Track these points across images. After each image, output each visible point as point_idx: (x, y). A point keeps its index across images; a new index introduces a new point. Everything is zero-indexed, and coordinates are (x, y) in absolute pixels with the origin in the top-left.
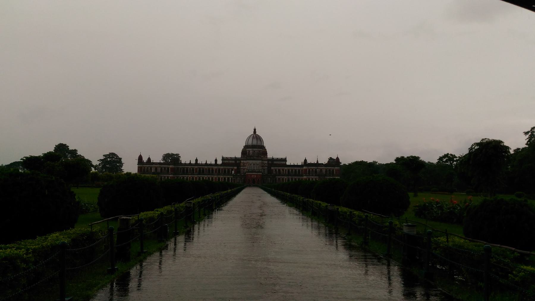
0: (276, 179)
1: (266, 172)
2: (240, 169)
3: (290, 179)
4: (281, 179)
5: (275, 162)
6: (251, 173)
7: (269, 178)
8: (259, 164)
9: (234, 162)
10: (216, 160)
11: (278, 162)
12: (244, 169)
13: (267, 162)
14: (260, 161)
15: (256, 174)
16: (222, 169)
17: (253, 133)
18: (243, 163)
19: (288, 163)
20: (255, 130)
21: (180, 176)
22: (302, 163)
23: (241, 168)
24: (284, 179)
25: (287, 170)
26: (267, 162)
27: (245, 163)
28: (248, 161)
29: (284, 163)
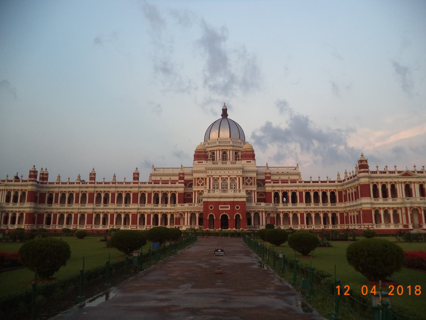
0: (278, 215)
1: (254, 196)
2: (192, 193)
3: (313, 215)
4: (291, 216)
7: (264, 214)
8: (236, 178)
9: (177, 178)
12: (200, 193)
16: (150, 194)
17: (221, 117)
18: (198, 178)
19: (304, 178)
22: (338, 175)
23: (194, 189)
24: (299, 215)
27: (202, 178)
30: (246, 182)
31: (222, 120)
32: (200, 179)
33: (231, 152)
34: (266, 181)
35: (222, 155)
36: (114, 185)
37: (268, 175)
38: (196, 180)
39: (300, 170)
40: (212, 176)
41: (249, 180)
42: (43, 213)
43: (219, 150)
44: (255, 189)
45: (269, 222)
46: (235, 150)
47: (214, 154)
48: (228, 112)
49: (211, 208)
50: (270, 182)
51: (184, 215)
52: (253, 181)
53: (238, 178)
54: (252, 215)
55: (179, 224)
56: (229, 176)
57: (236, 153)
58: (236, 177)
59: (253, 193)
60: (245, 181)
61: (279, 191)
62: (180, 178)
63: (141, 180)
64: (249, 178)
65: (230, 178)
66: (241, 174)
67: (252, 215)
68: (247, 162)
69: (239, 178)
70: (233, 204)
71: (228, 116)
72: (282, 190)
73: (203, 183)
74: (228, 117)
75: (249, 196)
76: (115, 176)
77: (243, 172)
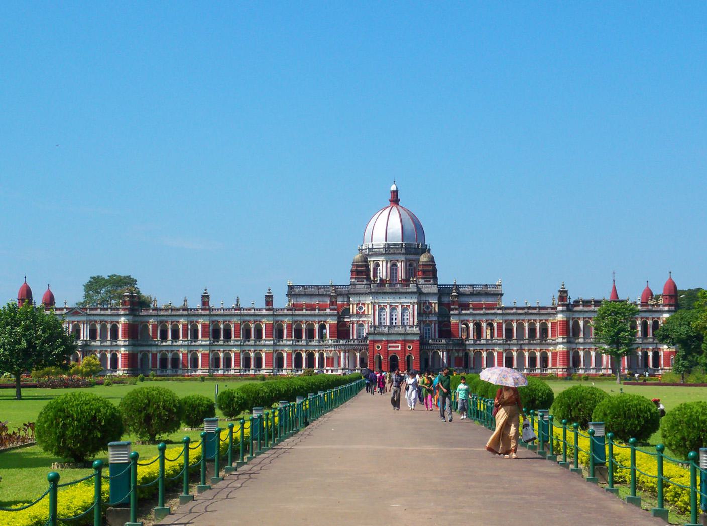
1: (434, 327)
10: (269, 299)
21: (154, 350)
22: (554, 299)
30: (424, 309)
31: (392, 208)
32: (360, 305)
34: (452, 307)
35: (390, 268)
36: (238, 312)
38: (355, 306)
41: (427, 306)
42: (136, 352)
44: (435, 318)
46: (410, 261)
47: (378, 265)
51: (340, 355)
53: (411, 306)
55: (333, 366)
57: (411, 265)
58: (409, 304)
59: (433, 324)
60: (422, 308)
62: (332, 303)
63: (276, 305)
64: (427, 303)
68: (425, 281)
71: (399, 200)
73: (364, 310)
76: (237, 300)
77: (419, 294)
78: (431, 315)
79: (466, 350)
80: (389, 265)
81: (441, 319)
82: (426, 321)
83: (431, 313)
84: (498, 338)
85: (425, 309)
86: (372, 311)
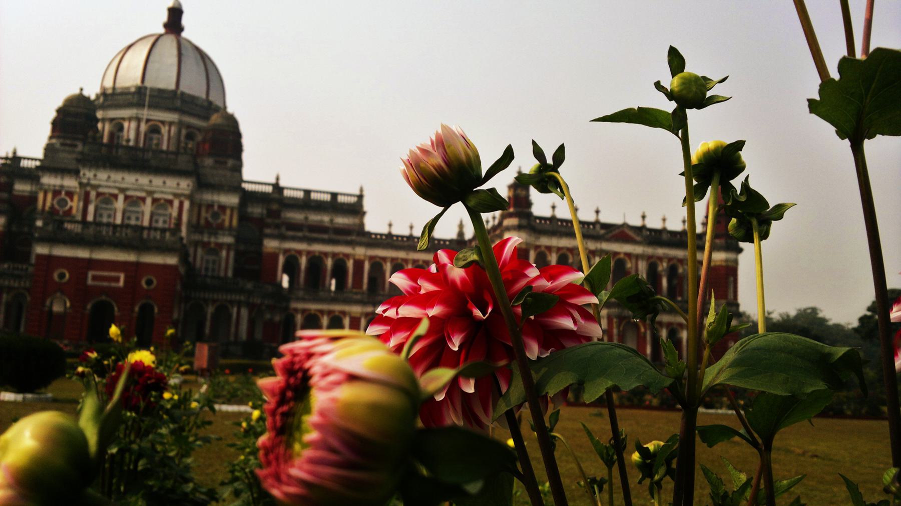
1: (226, 262)
5: (297, 216)
6: (83, 253)
8: (170, 202)
11: (315, 217)
13: (232, 200)
14: (185, 185)
15: (130, 257)
17: (162, 30)
18: (56, 193)
19: (374, 224)
20: (175, 15)
22: (461, 226)
25: (367, 266)
26: (232, 200)
27: (70, 194)
28: (88, 174)
29: (342, 220)
33: (174, 129)
37: (275, 207)
38: (50, 196)
39: (367, 205)
40: (95, 187)
43: (139, 120)
45: (259, 335)
47: (121, 128)
48: (185, 21)
49: (62, 276)
50: (277, 226)
52: (227, 218)
53: (176, 203)
54: (210, 310)
56: (150, 193)
57: (190, 137)
58: (170, 197)
60: (204, 214)
61: (300, 252)
65: (155, 201)
66: (187, 192)
67: (210, 310)
69: (181, 205)
70: (134, 270)
72: (308, 253)
74: (184, 34)
75: (211, 258)
78: (220, 232)
79: (287, 308)
80: (143, 127)
81: (242, 247)
82: (209, 243)
83: (221, 227)
84: (354, 290)
85: (210, 219)
86: (81, 204)
